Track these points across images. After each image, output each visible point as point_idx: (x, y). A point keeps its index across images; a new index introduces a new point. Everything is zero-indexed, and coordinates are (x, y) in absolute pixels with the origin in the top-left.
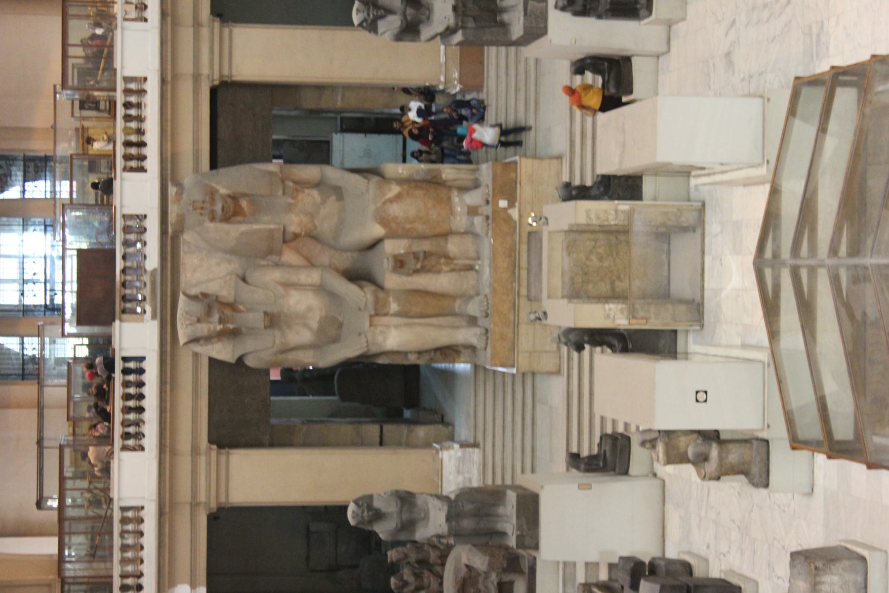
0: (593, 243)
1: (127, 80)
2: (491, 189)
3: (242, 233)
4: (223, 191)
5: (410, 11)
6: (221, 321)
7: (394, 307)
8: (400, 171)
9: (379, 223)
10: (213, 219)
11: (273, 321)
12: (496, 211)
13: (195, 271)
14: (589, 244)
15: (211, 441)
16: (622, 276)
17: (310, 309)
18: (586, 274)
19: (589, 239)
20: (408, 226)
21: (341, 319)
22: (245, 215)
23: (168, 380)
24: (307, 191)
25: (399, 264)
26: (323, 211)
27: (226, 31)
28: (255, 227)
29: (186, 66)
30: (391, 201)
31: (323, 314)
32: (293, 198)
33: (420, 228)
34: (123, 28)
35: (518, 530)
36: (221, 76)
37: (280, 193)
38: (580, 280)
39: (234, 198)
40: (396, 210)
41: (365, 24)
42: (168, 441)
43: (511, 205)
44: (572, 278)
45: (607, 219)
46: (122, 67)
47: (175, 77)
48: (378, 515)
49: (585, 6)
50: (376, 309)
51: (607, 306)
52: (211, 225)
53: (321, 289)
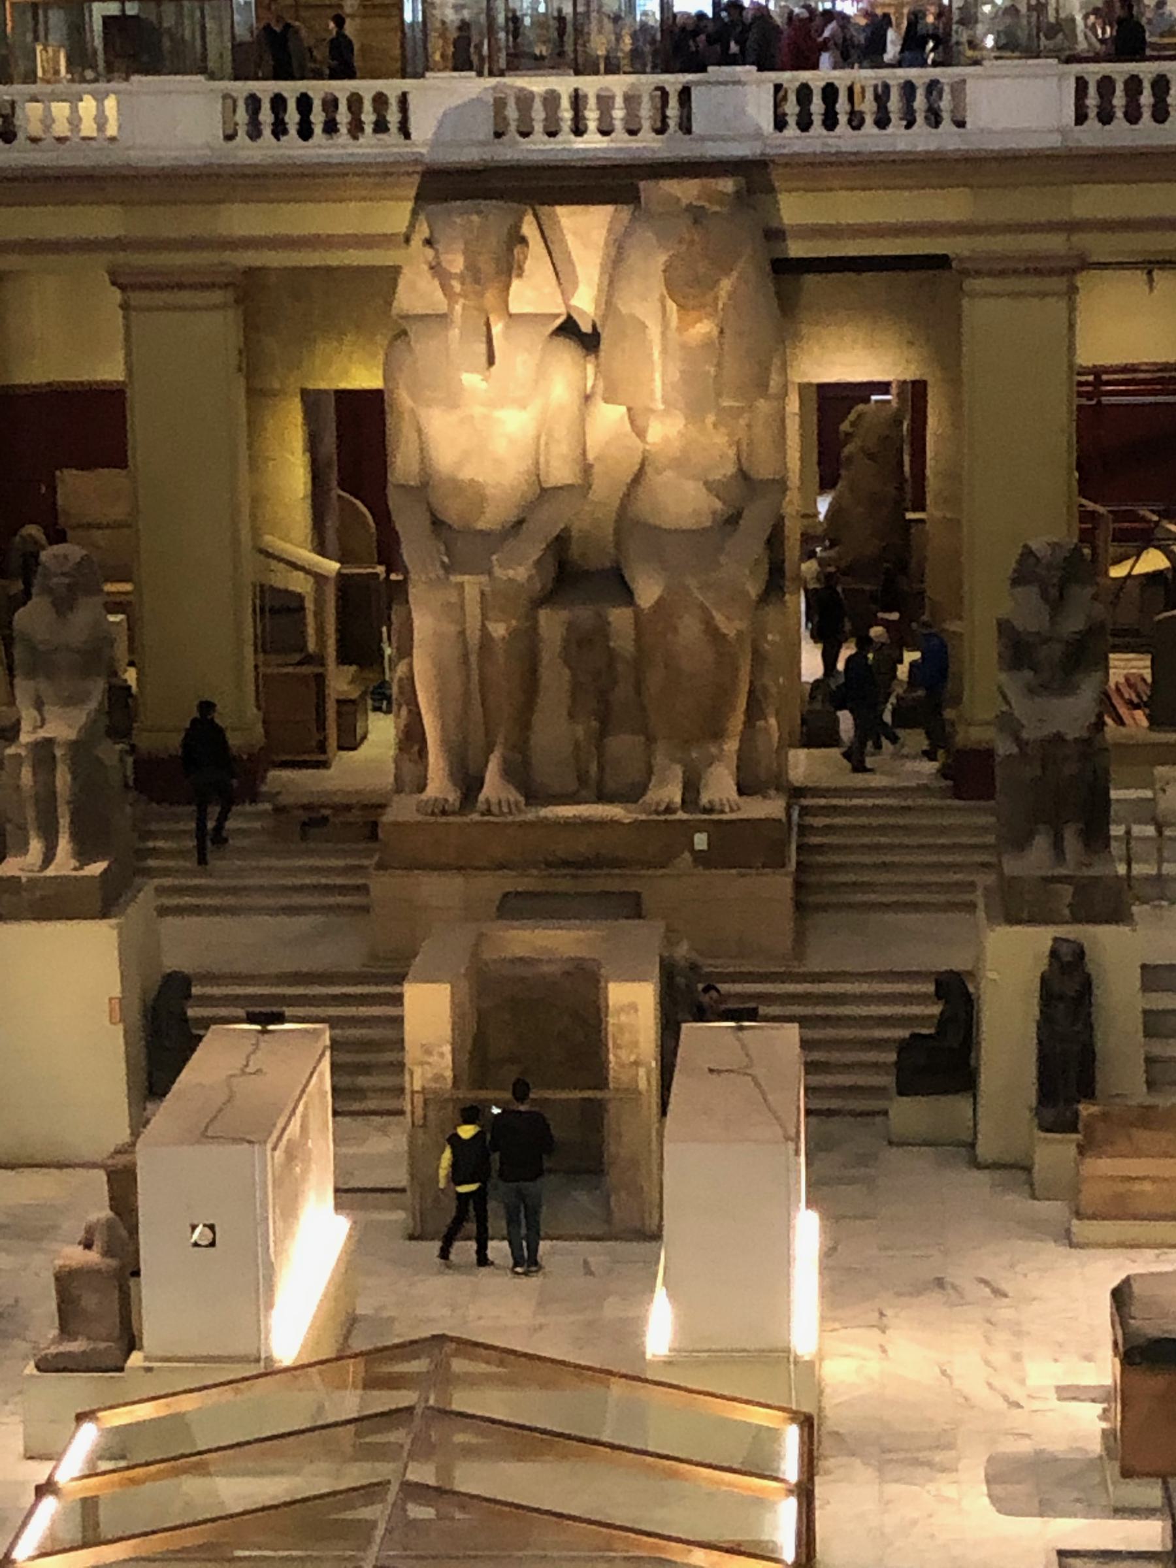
1: (959, 88)
2: (733, 816)
5: (1056, 650)
8: (770, 637)
12: (690, 828)
22: (680, 330)
31: (489, 491)
32: (715, 426)
33: (655, 679)
35: (30, 880)
40: (689, 629)
41: (1032, 560)
43: (702, 860)
45: (617, 1047)
48: (63, 604)
49: (1061, 998)
51: (447, 1049)
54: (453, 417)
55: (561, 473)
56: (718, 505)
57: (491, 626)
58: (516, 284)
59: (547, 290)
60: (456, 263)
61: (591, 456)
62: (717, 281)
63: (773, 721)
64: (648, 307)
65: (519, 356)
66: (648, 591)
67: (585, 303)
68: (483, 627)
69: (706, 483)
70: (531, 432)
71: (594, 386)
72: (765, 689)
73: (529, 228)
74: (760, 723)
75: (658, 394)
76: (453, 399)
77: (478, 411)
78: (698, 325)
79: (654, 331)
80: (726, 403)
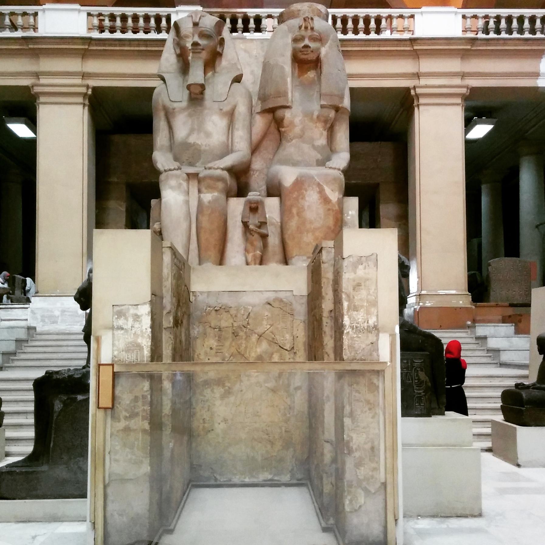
0: (288, 347)
3: (282, 68)
4: (324, 51)
6: (195, 44)
7: (207, 197)
8: (350, 213)
9: (297, 180)
10: (295, 40)
11: (196, 96)
13: (246, 51)
14: (286, 339)
15: (95, 89)
16: (232, 399)
17: (208, 135)
18: (235, 334)
19: (294, 338)
20: (294, 211)
21: (197, 164)
22: (299, 76)
23: (149, 49)
24: (325, 133)
25: (253, 206)
26: (306, 147)
27: (459, 101)
28: (289, 80)
29: (427, 65)
30: (321, 192)
31: (203, 148)
32: (318, 117)
33: (293, 224)
34: (456, 13)
36: (418, 96)
37: (323, 103)
38: (223, 324)
39: (316, 63)
40: (311, 197)
42: (95, 48)
44: (227, 309)
46: (422, 13)
47: (416, 55)
50: (205, 178)
52: (290, 40)
53: (227, 150)
68: (199, 197)
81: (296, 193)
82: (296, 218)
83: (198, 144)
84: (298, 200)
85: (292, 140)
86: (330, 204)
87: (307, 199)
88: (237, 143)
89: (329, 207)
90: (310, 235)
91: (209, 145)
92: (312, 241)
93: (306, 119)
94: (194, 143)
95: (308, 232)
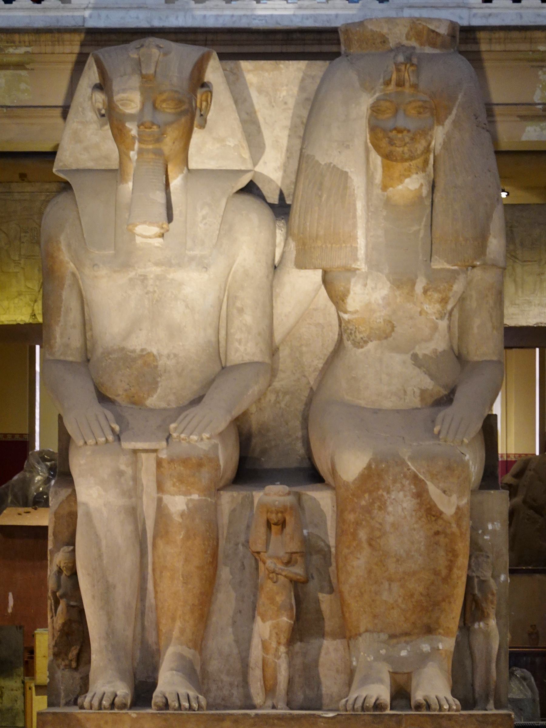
8: (490, 527)
20: (363, 535)
30: (421, 494)
32: (425, 291)
54: (122, 279)
55: (245, 348)
56: (428, 383)
57: (167, 499)
58: (197, 136)
59: (231, 143)
60: (131, 101)
61: (278, 337)
62: (431, 128)
63: (493, 622)
64: (351, 156)
65: (201, 213)
66: (351, 464)
67: (272, 169)
69: (415, 357)
70: (211, 298)
71: (282, 257)
72: (483, 583)
73: (214, 72)
74: (479, 625)
75: (361, 252)
76: (125, 258)
77: (154, 270)
78: (407, 180)
79: (358, 183)
80: (439, 264)
81: (367, 496)
82: (367, 550)
83: (149, 354)
84: (369, 512)
85: (366, 342)
86: (440, 522)
87: (390, 509)
88: (240, 341)
89: (436, 528)
90: (395, 587)
91: (175, 355)
92: (400, 600)
93: (397, 293)
94: (142, 350)
95: (390, 580)
